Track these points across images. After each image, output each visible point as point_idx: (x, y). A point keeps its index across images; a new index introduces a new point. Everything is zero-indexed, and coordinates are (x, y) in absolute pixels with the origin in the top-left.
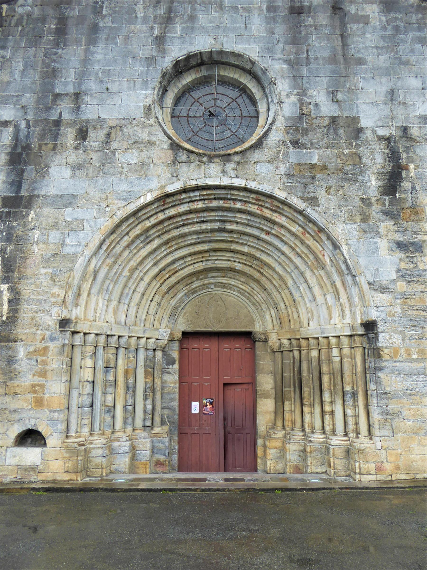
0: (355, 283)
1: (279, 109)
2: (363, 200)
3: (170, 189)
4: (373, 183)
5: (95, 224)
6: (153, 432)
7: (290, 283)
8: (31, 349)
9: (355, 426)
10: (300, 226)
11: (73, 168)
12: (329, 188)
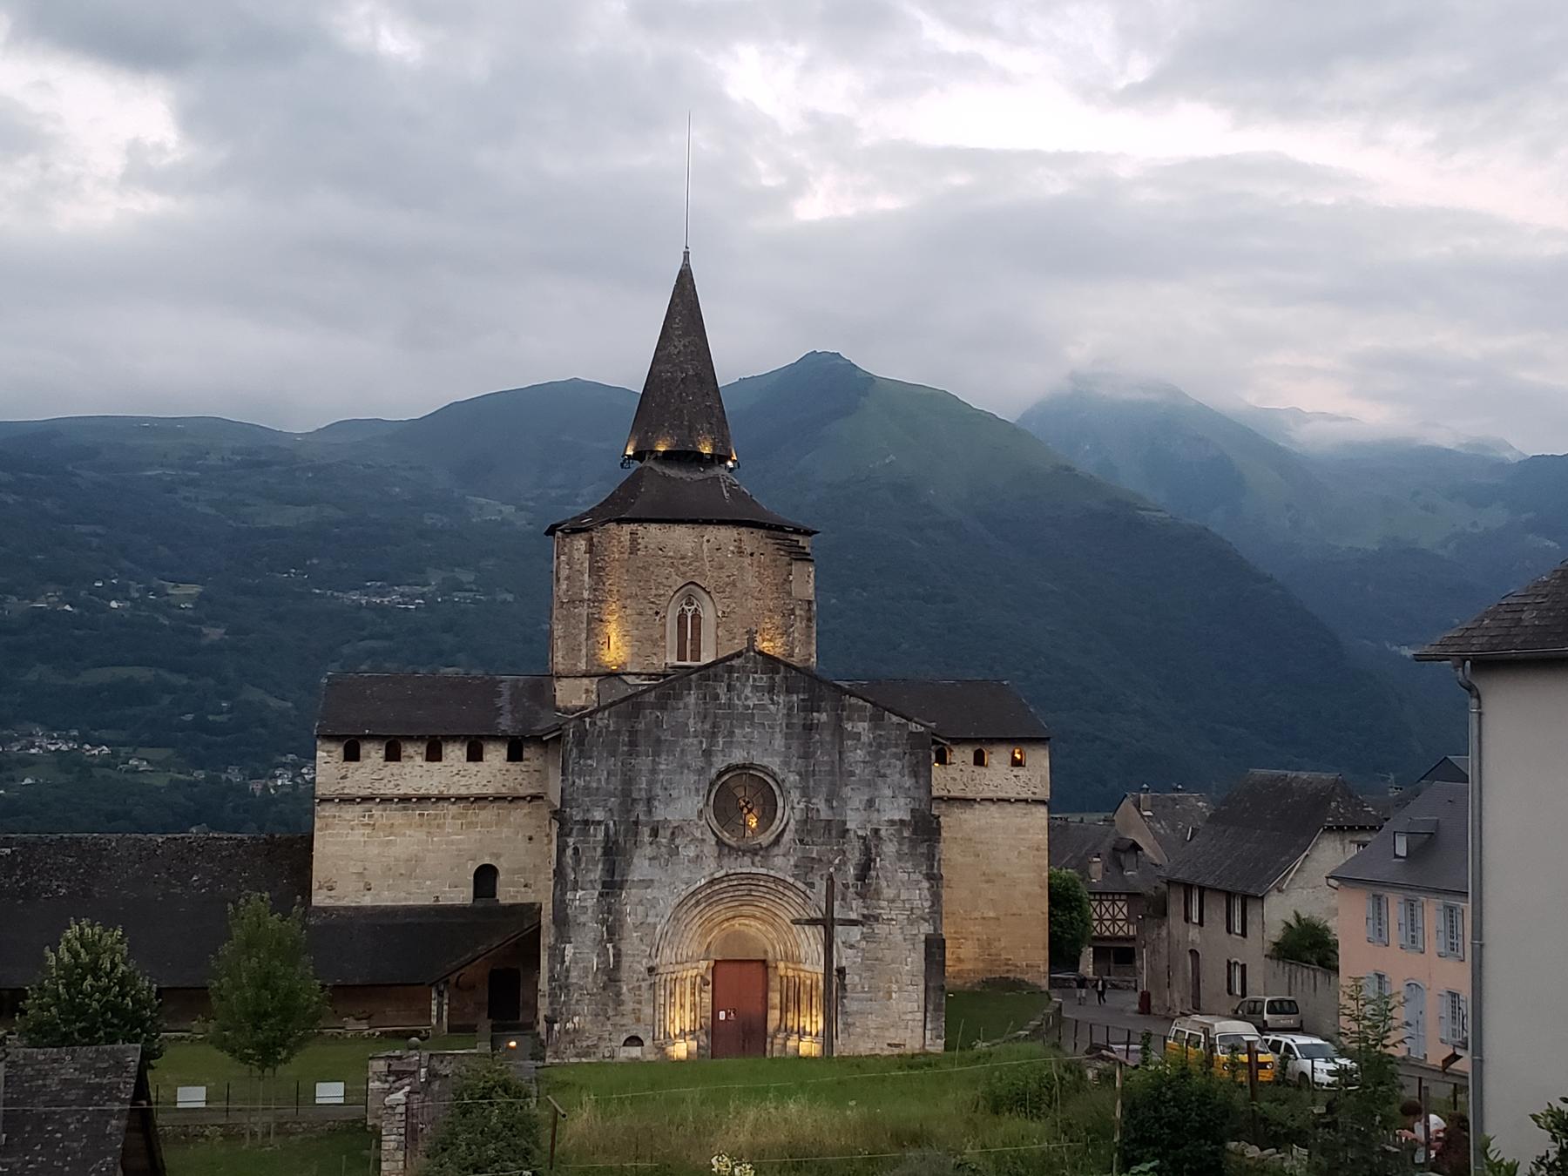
1: (790, 811)
3: (717, 875)
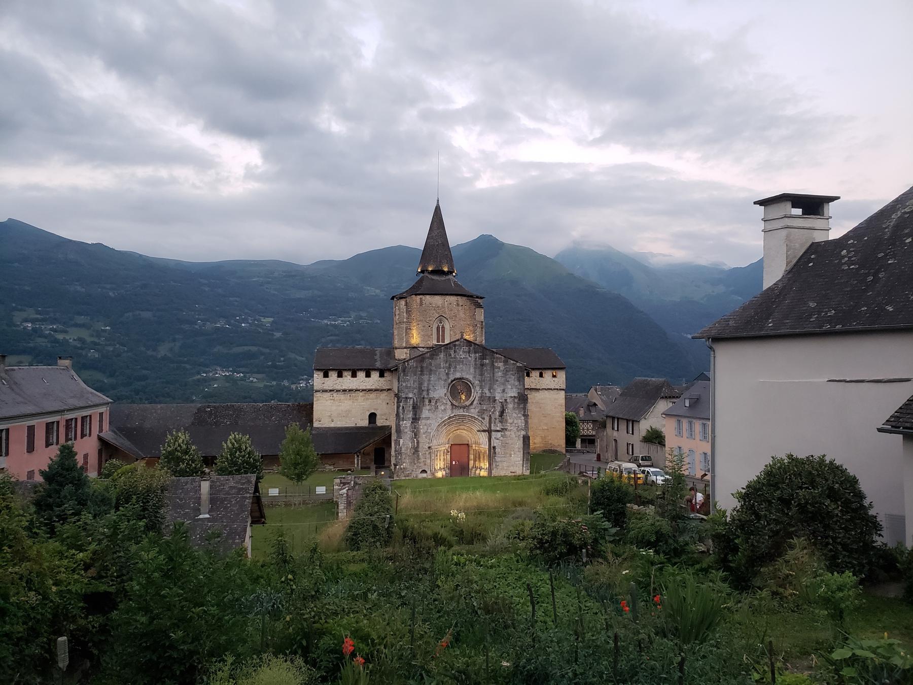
1: (476, 393)
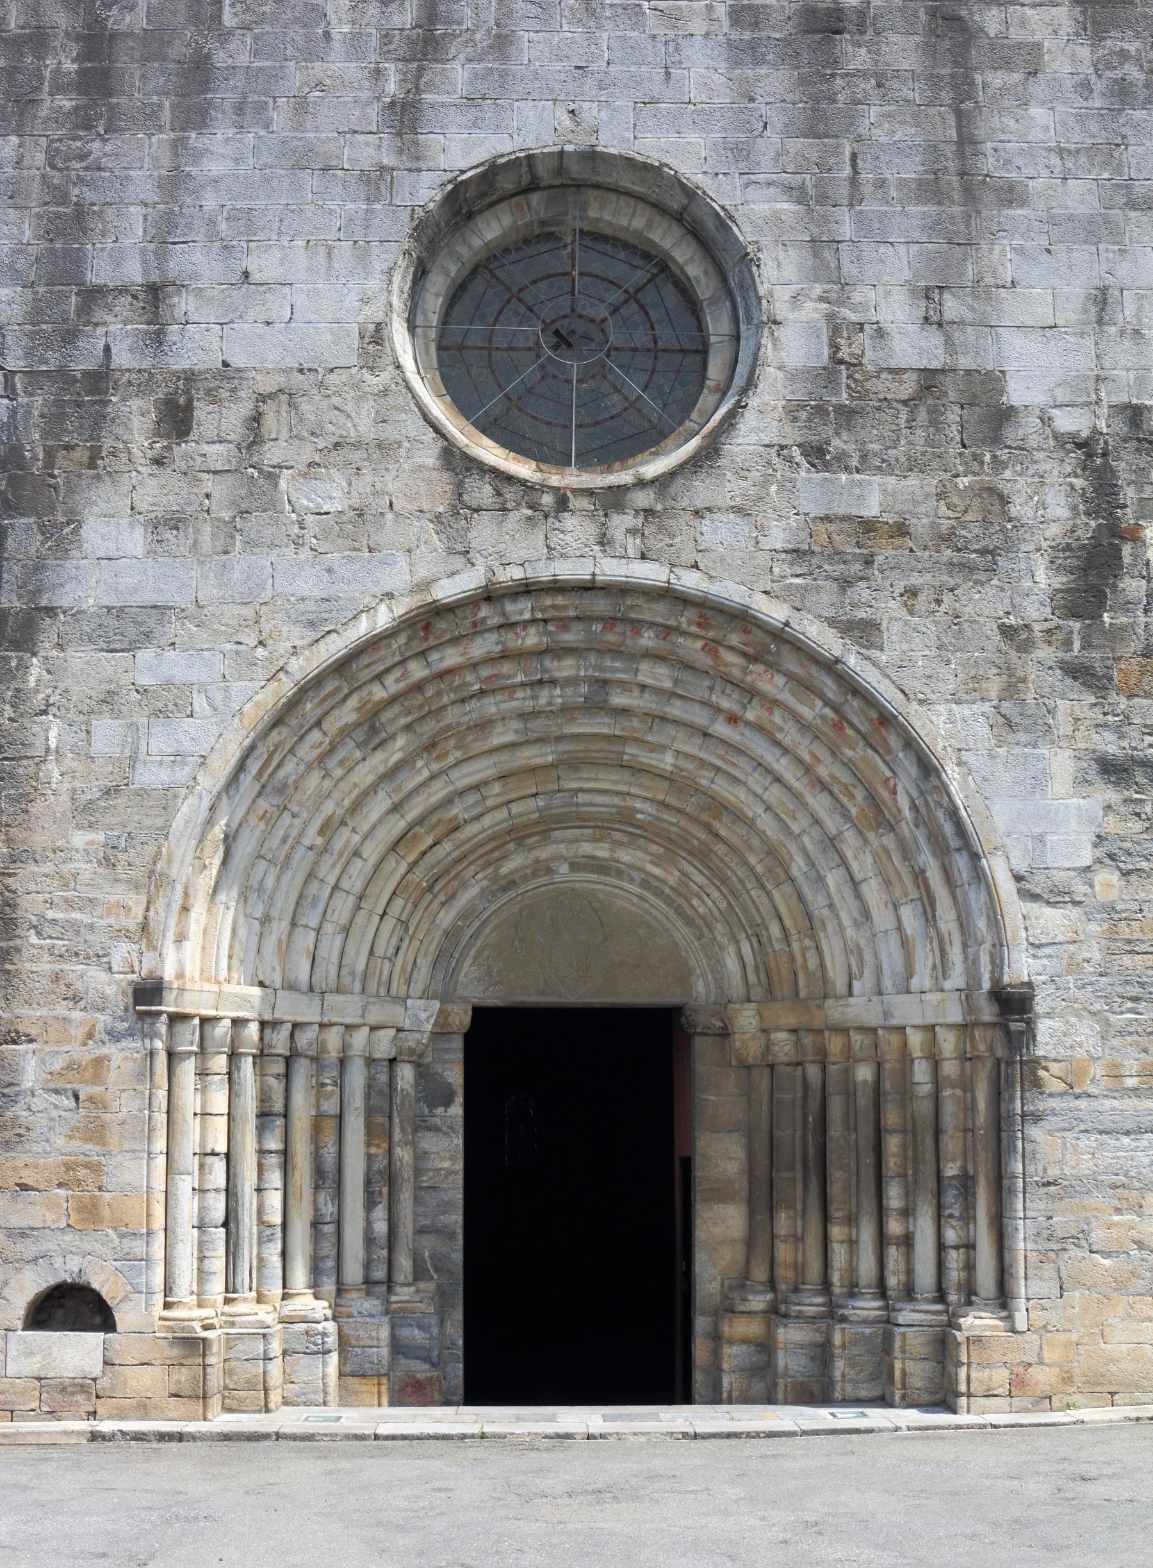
0: (980, 876)
2: (1007, 632)
3: (446, 591)
4: (1039, 580)
5: (227, 698)
6: (393, 1298)
7: (799, 865)
8: (58, 1064)
9: (963, 1275)
10: (827, 703)
11: (155, 525)
12: (912, 592)
